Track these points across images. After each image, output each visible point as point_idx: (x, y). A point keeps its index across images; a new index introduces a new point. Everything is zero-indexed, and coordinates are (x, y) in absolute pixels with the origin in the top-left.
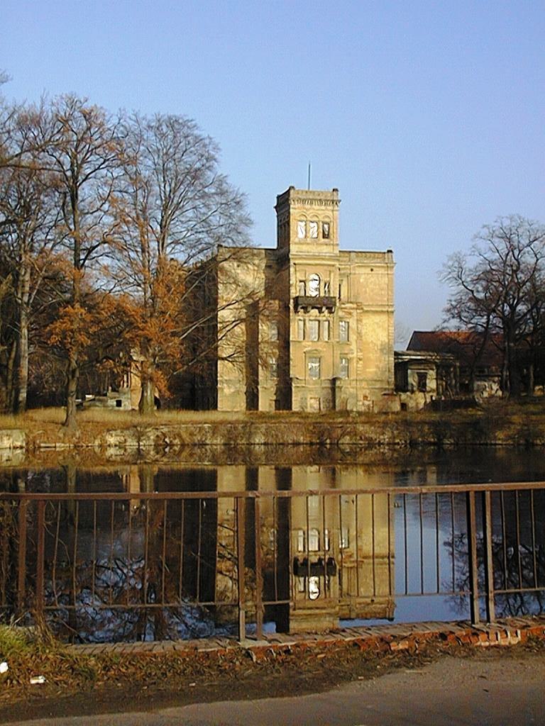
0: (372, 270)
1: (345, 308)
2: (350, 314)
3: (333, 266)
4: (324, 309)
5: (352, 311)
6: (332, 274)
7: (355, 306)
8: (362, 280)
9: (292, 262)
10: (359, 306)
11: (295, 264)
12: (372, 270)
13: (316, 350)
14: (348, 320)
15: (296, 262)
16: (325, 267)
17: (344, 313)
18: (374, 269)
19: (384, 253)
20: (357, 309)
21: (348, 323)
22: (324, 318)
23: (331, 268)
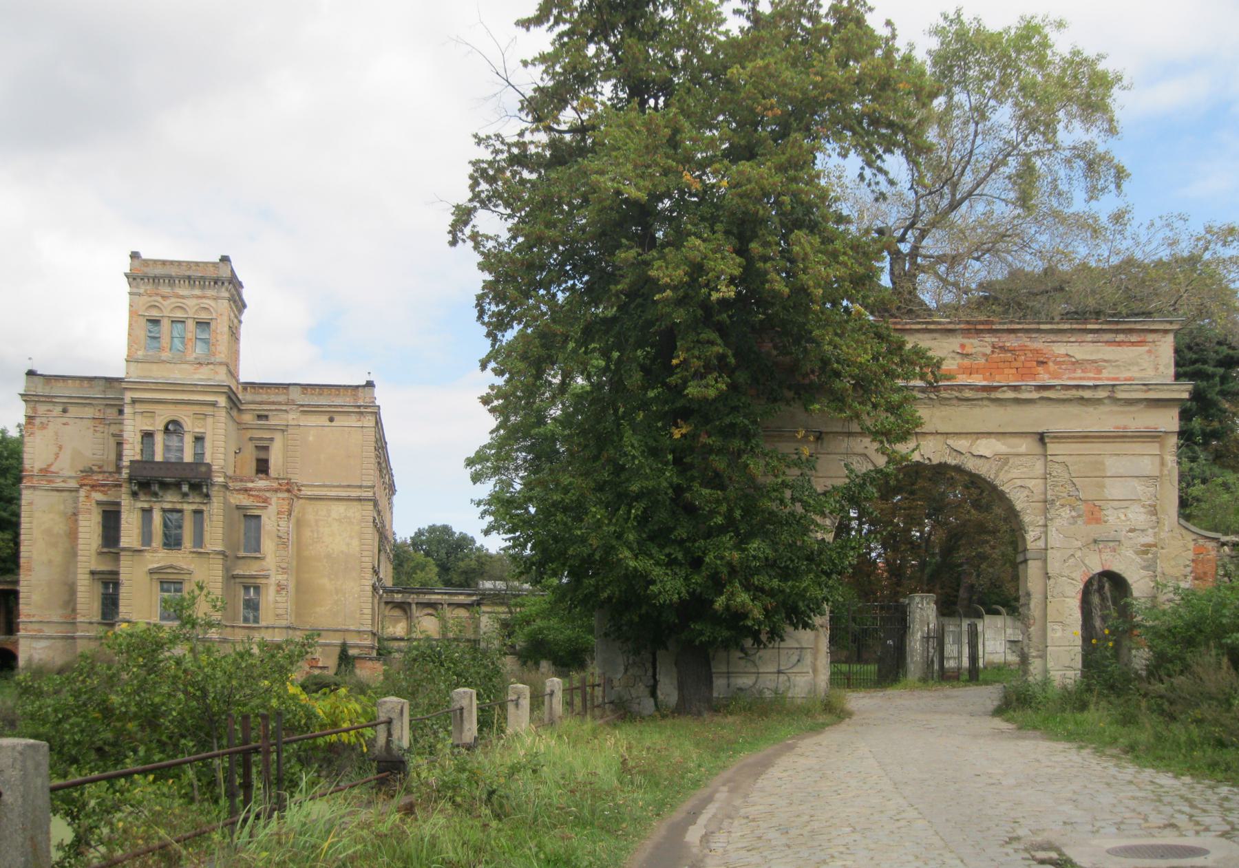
0: (331, 420)
1: (251, 489)
2: (266, 500)
3: (214, 404)
4: (185, 488)
5: (268, 494)
6: (210, 420)
7: (275, 485)
8: (311, 438)
9: (128, 396)
10: (289, 488)
11: (134, 401)
12: (331, 420)
13: (171, 567)
14: (257, 512)
15: (137, 395)
16: (197, 409)
17: (252, 499)
18: (336, 417)
19: (358, 387)
20: (276, 491)
21: (259, 517)
22: (194, 507)
23: (208, 410)
